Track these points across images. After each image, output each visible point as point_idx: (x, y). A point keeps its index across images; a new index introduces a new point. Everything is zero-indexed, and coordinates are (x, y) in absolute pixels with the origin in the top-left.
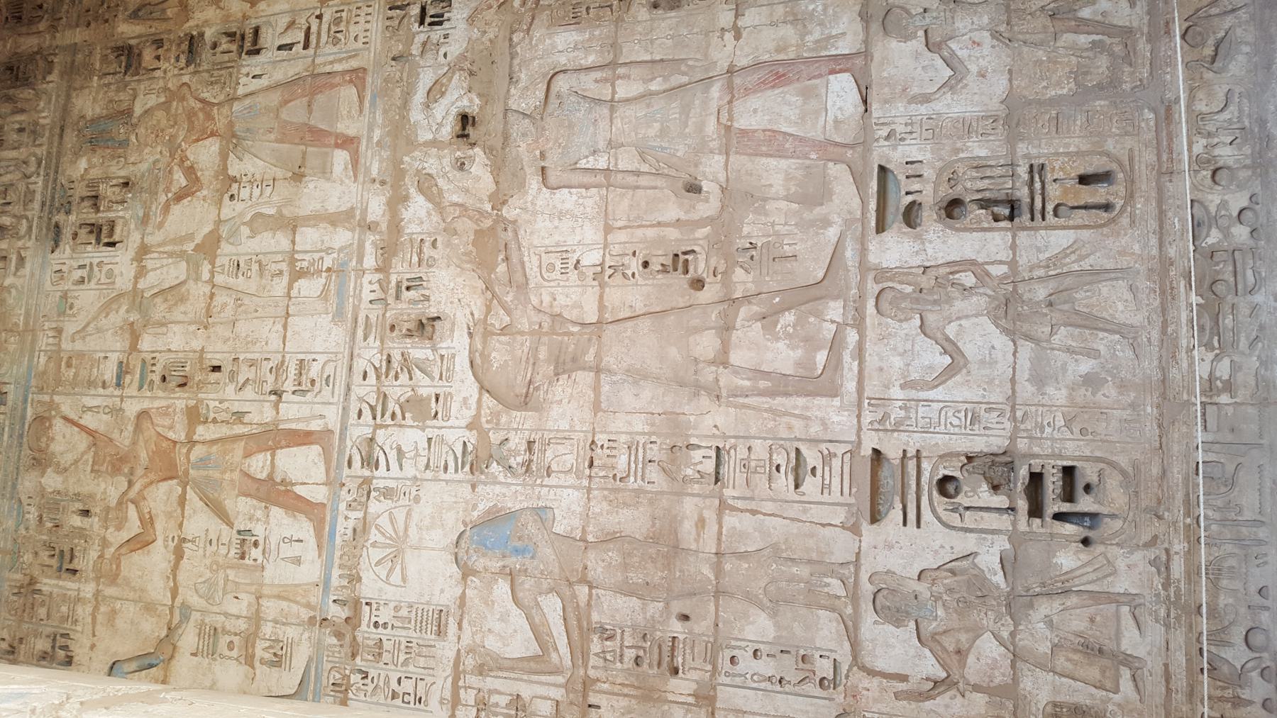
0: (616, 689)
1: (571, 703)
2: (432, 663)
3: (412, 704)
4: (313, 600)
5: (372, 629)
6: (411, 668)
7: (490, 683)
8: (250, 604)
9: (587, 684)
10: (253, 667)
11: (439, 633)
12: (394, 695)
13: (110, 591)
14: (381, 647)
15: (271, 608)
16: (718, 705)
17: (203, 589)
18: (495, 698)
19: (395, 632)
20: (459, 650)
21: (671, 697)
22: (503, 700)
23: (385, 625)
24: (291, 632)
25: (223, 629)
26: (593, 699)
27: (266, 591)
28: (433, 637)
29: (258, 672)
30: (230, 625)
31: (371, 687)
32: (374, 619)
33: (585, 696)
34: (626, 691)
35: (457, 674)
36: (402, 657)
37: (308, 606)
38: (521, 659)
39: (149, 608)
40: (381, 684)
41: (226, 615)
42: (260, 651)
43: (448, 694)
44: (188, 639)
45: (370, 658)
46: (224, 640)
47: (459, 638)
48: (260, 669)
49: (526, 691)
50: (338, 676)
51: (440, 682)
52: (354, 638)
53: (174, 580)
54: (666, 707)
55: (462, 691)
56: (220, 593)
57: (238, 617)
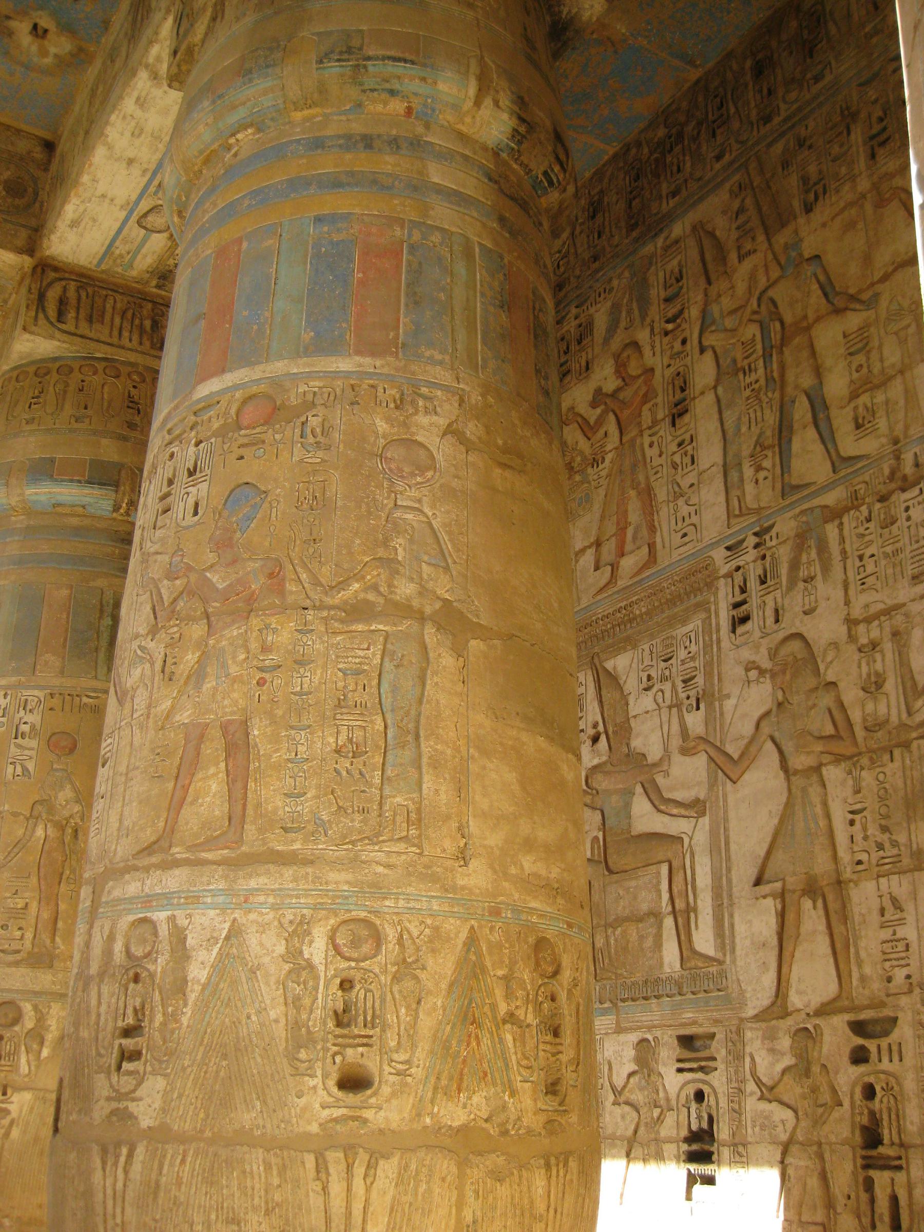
0: (908, 773)
1: (890, 733)
2: (891, 581)
3: (859, 577)
4: (912, 431)
5: (903, 506)
6: (883, 562)
7: (888, 646)
8: (893, 365)
9: (906, 745)
10: (850, 402)
11: (914, 578)
12: (861, 558)
13: (869, 207)
14: (892, 523)
15: (896, 390)
16: (916, 873)
17: (894, 306)
18: (878, 656)
19: (906, 530)
20: (904, 605)
21: (913, 827)
22: (879, 666)
23: (908, 519)
24: (882, 423)
25: (869, 352)
26: (897, 752)
27: (908, 375)
28: (910, 572)
29: (848, 409)
30: (874, 355)
31: (861, 530)
32: (910, 503)
33: (898, 746)
34: (909, 782)
35: (888, 612)
36: (889, 549)
37: (907, 428)
38: (911, 671)
39: (867, 260)
40: (867, 538)
41: (880, 347)
42: (864, 399)
43: (873, 610)
44: (853, 320)
45: (882, 516)
46: (860, 359)
47: (913, 600)
48: (848, 412)
49: (890, 685)
50: (862, 492)
51: (878, 597)
52: (893, 492)
53: (895, 270)
54: (905, 825)
55: (876, 623)
56: (895, 329)
57: (882, 360)
